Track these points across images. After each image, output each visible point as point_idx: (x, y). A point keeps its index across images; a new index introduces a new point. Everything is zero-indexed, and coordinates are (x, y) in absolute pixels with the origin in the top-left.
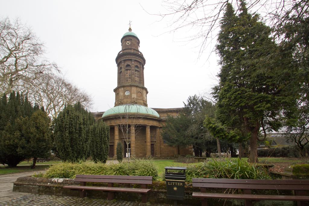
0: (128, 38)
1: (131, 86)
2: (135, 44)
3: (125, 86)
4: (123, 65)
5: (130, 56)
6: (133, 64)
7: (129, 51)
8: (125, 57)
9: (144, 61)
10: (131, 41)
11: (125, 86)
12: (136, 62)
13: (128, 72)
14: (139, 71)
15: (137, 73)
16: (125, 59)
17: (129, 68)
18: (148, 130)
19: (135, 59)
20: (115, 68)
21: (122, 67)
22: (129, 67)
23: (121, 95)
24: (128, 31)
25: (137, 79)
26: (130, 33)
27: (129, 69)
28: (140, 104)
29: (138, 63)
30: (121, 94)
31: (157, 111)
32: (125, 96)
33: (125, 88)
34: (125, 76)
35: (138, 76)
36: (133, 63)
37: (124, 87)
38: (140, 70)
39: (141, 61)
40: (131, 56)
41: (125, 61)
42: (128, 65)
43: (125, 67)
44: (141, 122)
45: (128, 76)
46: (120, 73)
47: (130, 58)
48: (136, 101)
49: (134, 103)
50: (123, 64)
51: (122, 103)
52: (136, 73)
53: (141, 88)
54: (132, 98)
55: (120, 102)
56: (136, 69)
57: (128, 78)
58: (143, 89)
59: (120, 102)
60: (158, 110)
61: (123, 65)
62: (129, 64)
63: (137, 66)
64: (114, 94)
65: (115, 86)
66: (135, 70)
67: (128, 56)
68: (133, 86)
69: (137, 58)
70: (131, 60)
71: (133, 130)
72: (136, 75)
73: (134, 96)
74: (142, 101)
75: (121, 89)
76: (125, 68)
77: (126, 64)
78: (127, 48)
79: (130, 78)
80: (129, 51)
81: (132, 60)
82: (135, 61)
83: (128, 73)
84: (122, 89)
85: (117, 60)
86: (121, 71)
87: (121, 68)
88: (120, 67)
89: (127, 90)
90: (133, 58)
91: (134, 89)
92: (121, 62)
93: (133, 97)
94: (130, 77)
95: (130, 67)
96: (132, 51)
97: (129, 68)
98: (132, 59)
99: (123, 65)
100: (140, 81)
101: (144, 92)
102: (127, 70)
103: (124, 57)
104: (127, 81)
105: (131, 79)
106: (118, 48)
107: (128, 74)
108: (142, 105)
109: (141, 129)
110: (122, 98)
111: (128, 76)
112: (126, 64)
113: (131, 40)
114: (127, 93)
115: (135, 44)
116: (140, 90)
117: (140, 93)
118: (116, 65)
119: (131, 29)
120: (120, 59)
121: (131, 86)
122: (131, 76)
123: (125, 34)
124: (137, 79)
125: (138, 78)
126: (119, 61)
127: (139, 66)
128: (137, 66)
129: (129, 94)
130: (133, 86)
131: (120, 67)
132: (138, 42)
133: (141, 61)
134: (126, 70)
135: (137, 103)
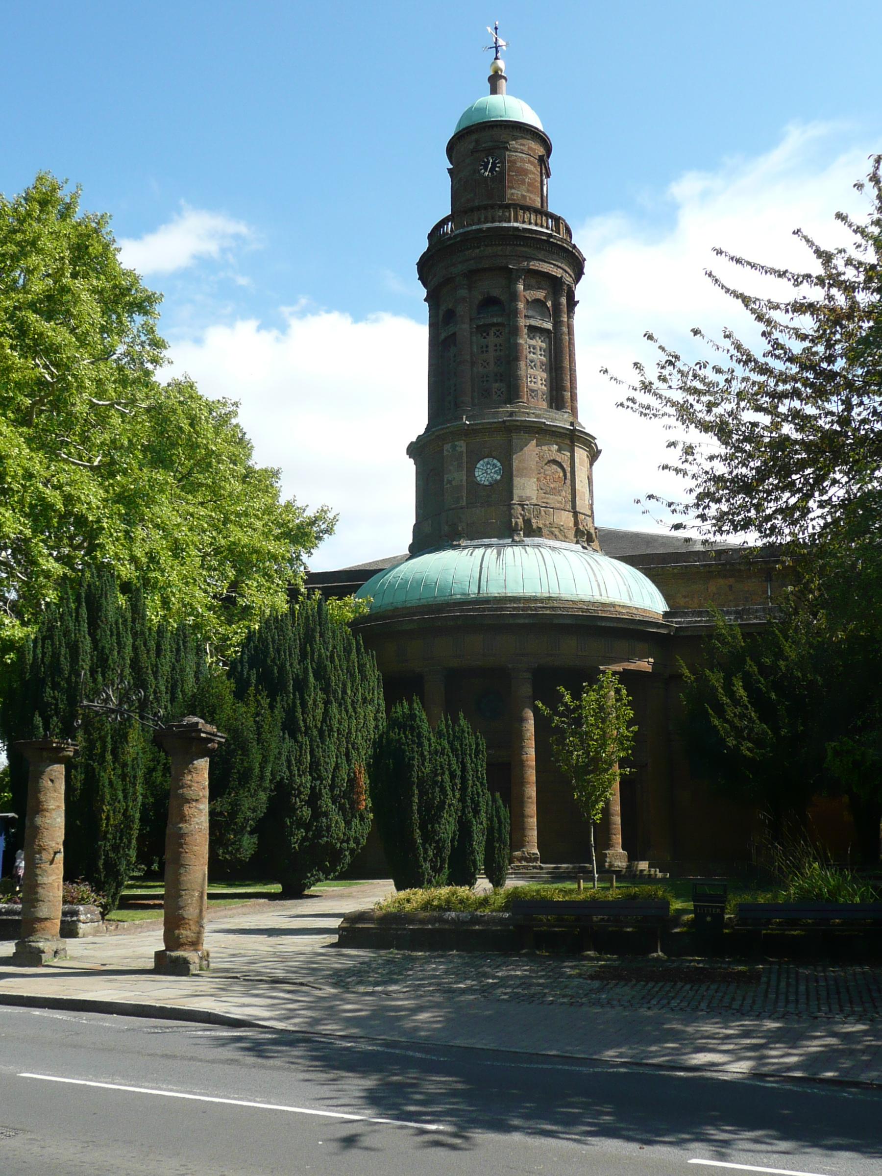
13: (492, 340)
21: (461, 310)
23: (454, 483)
27: (494, 325)
28: (557, 533)
42: (490, 302)
50: (463, 292)
52: (533, 342)
56: (533, 322)
62: (496, 293)
64: (409, 467)
65: (416, 420)
75: (454, 447)
76: (471, 320)
83: (491, 349)
84: (462, 446)
86: (454, 334)
88: (443, 308)
92: (448, 281)
101: (581, 454)
102: (484, 330)
108: (565, 539)
118: (424, 292)
129: (499, 477)
131: (443, 308)
132: (541, 151)
134: (478, 327)
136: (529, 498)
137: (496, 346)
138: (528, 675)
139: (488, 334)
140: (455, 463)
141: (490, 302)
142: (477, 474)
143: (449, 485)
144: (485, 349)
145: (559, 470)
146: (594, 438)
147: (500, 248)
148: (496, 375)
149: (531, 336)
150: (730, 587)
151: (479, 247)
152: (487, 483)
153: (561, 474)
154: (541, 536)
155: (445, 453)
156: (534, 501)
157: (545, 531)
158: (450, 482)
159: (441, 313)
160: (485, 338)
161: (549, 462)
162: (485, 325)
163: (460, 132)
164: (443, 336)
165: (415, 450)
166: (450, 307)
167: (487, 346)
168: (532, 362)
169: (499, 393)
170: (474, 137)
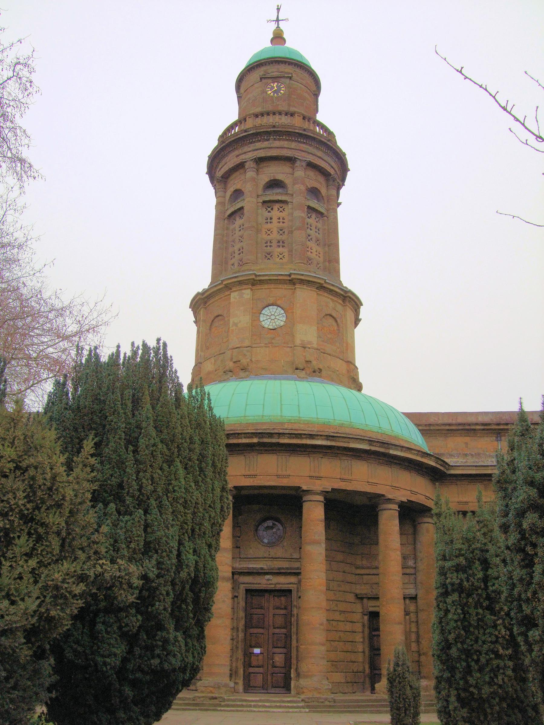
0: (273, 70)
1: (292, 282)
2: (306, 95)
3: (262, 282)
4: (251, 182)
5: (285, 144)
6: (298, 179)
7: (284, 120)
8: (266, 144)
9: (344, 169)
10: (288, 81)
11: (262, 282)
12: (311, 173)
13: (275, 213)
14: (321, 214)
15: (313, 220)
16: (262, 154)
17: (280, 198)
18: (389, 522)
19: (310, 158)
20: (203, 201)
21: (247, 188)
22: (279, 190)
24: (270, 45)
25: (315, 251)
26: (279, 52)
29: (321, 179)
30: (240, 318)
31: (417, 425)
32: (257, 330)
33: (263, 292)
34: (258, 231)
35: (320, 236)
36: (300, 173)
37: (255, 282)
38: (328, 210)
39: (332, 172)
40: (293, 145)
41: (260, 161)
42: (274, 184)
43: (260, 192)
44: (363, 478)
45: (275, 236)
46: (228, 216)
47: (289, 153)
48: (314, 363)
49: (308, 369)
50: (250, 174)
51: (244, 369)
52: (309, 221)
53: (336, 294)
54: (298, 342)
55: (231, 365)
57: (274, 244)
58: (344, 301)
59: (231, 365)
60: (424, 422)
61: (251, 182)
62: (280, 177)
63: (314, 192)
65: (203, 280)
66: (309, 207)
67: (277, 144)
68: (302, 282)
69: (319, 154)
70: (291, 160)
71: (314, 513)
72: (312, 233)
73: (307, 334)
74: (340, 366)
77: (264, 178)
78: (269, 107)
79: (281, 243)
80: (284, 120)
81: (298, 163)
82: (311, 165)
83: (275, 220)
84: (247, 293)
85: (215, 160)
86: (242, 208)
87: (238, 194)
89: (271, 300)
90: (306, 152)
91: (305, 296)
93: (299, 338)
94: (284, 237)
95: (287, 194)
96: (297, 122)
97: (281, 194)
98: (297, 154)
99: (253, 179)
100: (330, 261)
101: (350, 315)
103: (258, 145)
104: (269, 256)
105: (291, 251)
106: (226, 111)
107: (275, 226)
109: (352, 516)
110: (247, 343)
111: (275, 236)
112: (267, 180)
113: (290, 78)
114: (273, 318)
115: (306, 95)
116: (331, 304)
117: (331, 321)
119: (285, 36)
120: (224, 165)
121: (292, 282)
122: (291, 232)
123: (262, 52)
124: (315, 251)
125: (320, 249)
126: (231, 161)
127: (323, 191)
128: (314, 192)
130: (302, 282)
132: (314, 88)
133: (329, 167)
134: (264, 202)
135: (320, 370)
136: (310, 343)
137: (279, 219)
138: (321, 498)
139: (272, 209)
140: (242, 308)
141: (274, 184)
142: (261, 319)
143: (234, 328)
144: (269, 220)
145: (334, 323)
146: (362, 305)
147: (286, 142)
148: (279, 242)
149: (309, 215)
150: (466, 444)
151: (268, 140)
152: (271, 327)
153: (336, 328)
154: (320, 377)
155: (232, 300)
156: (315, 346)
157: (324, 373)
158: (236, 324)
159: (229, 193)
160: (269, 212)
161: (326, 315)
162: (270, 201)
163: (251, 64)
164: (229, 212)
165: (200, 303)
166: (238, 187)
167: (271, 219)
168: (309, 236)
169: (281, 256)
170: (263, 69)
